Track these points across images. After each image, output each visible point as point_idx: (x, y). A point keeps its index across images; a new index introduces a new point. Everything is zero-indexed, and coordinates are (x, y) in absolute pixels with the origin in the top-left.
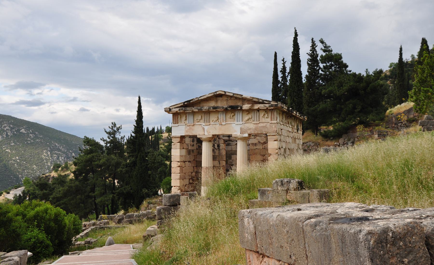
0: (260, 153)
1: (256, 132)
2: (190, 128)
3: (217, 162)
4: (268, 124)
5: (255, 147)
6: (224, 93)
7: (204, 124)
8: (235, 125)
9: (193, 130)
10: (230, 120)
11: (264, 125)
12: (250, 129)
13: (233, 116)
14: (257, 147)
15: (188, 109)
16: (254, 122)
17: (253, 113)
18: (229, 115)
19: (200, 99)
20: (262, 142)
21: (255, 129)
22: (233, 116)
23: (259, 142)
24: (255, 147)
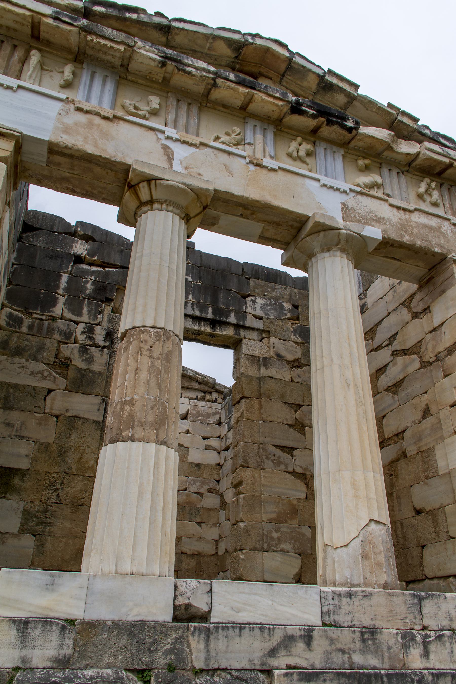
0: (283, 396)
1: (406, 239)
2: (90, 124)
3: (97, 400)
4: (446, 223)
5: (264, 372)
6: (287, 54)
7: (171, 132)
8: (316, 184)
9: (106, 135)
10: (289, 160)
11: (434, 222)
12: (379, 220)
13: (308, 154)
14: (273, 372)
15: (108, 31)
16: (391, 201)
17: (385, 171)
18: (294, 146)
19: (175, 24)
20: (290, 357)
21: (403, 226)
22: (308, 154)
23: (279, 356)
24: (264, 372)
